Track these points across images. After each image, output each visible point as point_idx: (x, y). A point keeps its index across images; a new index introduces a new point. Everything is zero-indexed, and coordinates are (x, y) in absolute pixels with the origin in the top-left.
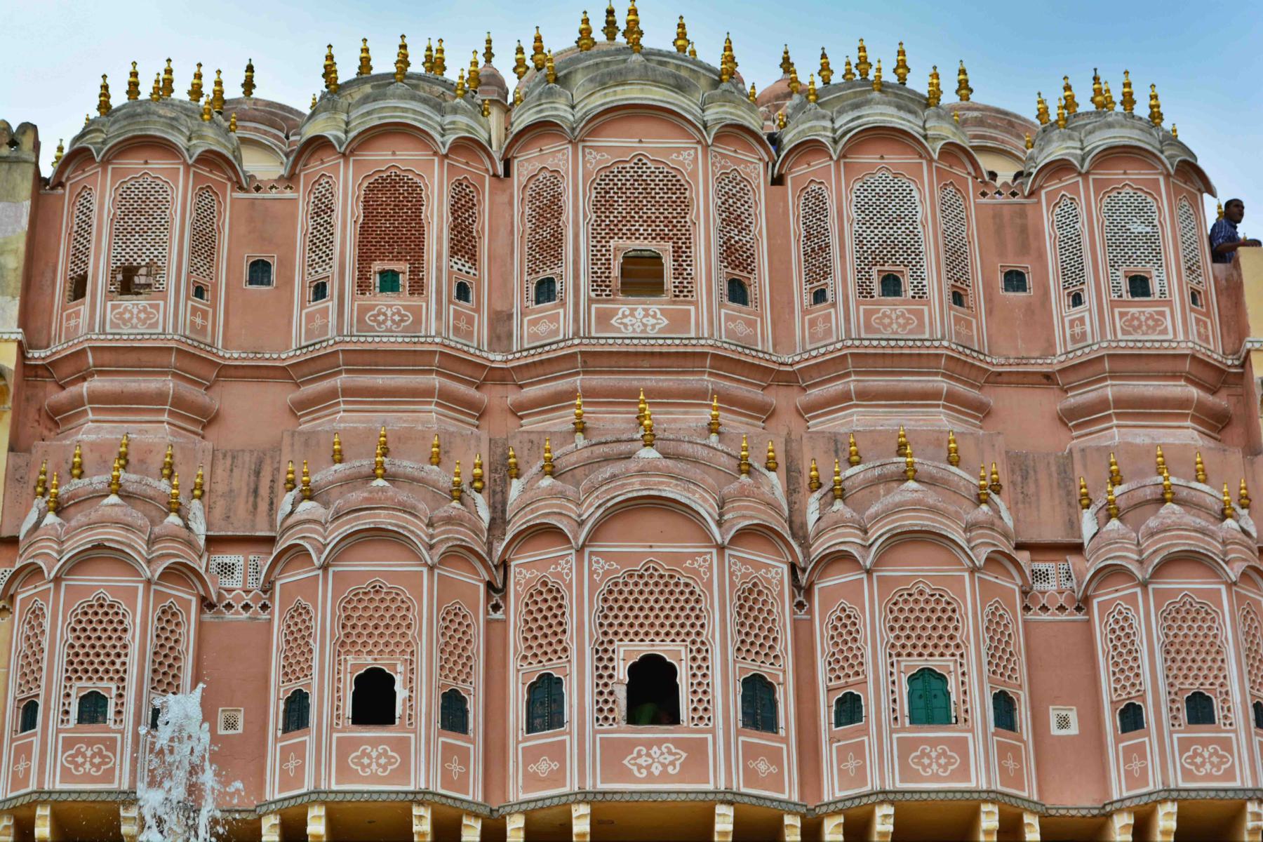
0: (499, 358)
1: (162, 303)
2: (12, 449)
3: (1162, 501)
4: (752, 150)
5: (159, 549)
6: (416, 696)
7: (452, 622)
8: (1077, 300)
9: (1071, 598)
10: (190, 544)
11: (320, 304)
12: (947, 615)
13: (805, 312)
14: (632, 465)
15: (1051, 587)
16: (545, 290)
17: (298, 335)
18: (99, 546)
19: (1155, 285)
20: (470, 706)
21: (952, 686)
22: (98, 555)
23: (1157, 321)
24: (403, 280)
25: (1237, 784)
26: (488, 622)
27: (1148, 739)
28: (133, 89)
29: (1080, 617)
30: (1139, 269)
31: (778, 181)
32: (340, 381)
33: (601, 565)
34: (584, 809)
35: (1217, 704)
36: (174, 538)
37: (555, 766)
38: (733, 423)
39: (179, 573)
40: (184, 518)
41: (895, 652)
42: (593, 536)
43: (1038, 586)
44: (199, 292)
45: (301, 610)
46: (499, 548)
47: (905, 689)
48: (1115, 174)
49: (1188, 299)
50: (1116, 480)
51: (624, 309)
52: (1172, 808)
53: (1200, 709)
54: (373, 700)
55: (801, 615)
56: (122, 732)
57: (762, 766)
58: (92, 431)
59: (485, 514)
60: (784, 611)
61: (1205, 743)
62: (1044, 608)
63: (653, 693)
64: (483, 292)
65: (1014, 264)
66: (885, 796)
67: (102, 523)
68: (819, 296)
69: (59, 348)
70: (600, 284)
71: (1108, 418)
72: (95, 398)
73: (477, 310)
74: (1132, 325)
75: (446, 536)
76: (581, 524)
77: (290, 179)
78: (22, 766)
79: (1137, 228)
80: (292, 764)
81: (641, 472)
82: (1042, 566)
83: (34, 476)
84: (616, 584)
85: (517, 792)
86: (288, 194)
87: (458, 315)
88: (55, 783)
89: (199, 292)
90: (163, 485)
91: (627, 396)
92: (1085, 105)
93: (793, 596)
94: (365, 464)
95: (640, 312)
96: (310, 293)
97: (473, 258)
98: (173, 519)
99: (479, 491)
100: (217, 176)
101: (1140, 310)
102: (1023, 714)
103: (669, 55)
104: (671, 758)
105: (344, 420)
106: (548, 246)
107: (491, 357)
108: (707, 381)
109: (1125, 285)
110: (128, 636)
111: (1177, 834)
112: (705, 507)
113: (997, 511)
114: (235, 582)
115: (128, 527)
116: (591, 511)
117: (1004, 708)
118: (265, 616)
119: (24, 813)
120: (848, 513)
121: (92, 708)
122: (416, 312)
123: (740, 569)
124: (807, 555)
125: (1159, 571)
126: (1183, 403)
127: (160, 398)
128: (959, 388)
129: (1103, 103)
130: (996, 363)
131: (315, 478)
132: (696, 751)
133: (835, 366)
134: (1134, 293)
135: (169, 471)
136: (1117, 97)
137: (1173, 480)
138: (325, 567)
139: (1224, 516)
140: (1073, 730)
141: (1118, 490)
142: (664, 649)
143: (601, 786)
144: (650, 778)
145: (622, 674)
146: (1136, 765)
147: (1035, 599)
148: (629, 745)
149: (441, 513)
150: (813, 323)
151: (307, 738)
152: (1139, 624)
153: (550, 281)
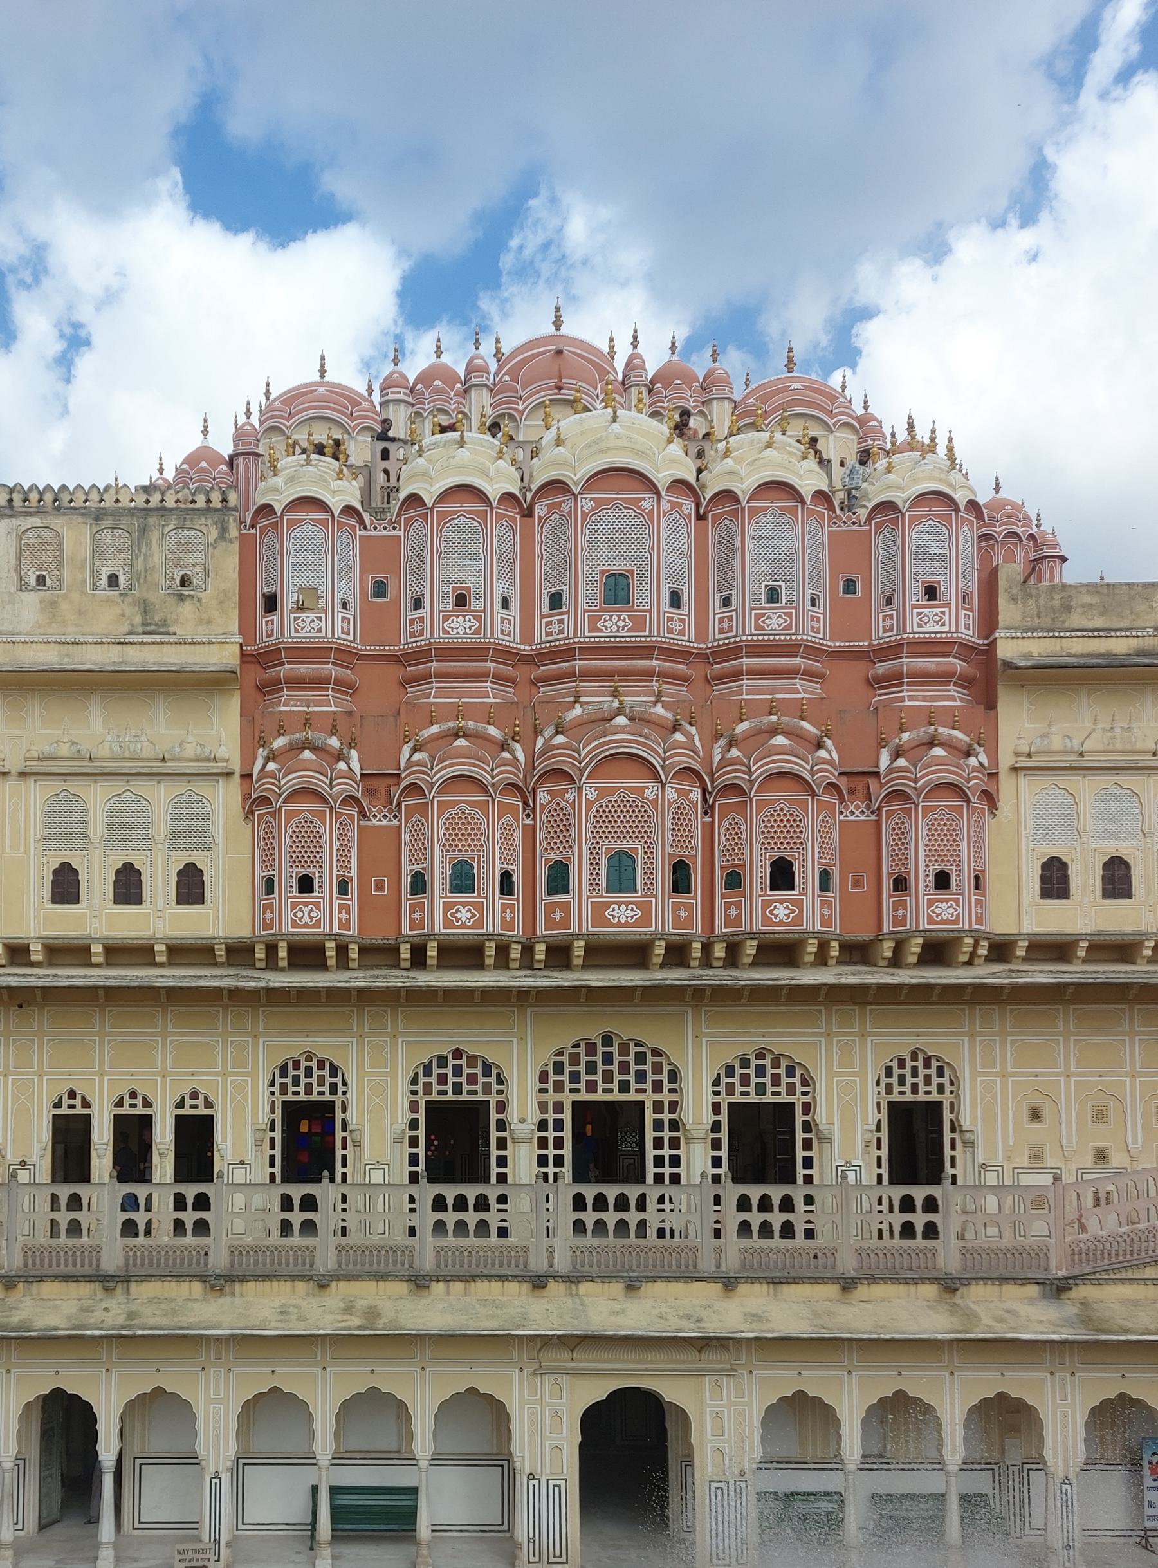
0: (527, 648)
1: (323, 616)
20: (515, 879)
40: (348, 764)
54: (463, 879)
56: (323, 898)
59: (521, 757)
63: (622, 873)
66: (751, 935)
69: (263, 641)
78: (268, 916)
80: (417, 915)
84: (601, 806)
88: (287, 928)
93: (703, 807)
99: (517, 742)
104: (632, 913)
107: (522, 647)
110: (322, 842)
118: (395, 822)
121: (306, 884)
132: (645, 908)
144: (619, 925)
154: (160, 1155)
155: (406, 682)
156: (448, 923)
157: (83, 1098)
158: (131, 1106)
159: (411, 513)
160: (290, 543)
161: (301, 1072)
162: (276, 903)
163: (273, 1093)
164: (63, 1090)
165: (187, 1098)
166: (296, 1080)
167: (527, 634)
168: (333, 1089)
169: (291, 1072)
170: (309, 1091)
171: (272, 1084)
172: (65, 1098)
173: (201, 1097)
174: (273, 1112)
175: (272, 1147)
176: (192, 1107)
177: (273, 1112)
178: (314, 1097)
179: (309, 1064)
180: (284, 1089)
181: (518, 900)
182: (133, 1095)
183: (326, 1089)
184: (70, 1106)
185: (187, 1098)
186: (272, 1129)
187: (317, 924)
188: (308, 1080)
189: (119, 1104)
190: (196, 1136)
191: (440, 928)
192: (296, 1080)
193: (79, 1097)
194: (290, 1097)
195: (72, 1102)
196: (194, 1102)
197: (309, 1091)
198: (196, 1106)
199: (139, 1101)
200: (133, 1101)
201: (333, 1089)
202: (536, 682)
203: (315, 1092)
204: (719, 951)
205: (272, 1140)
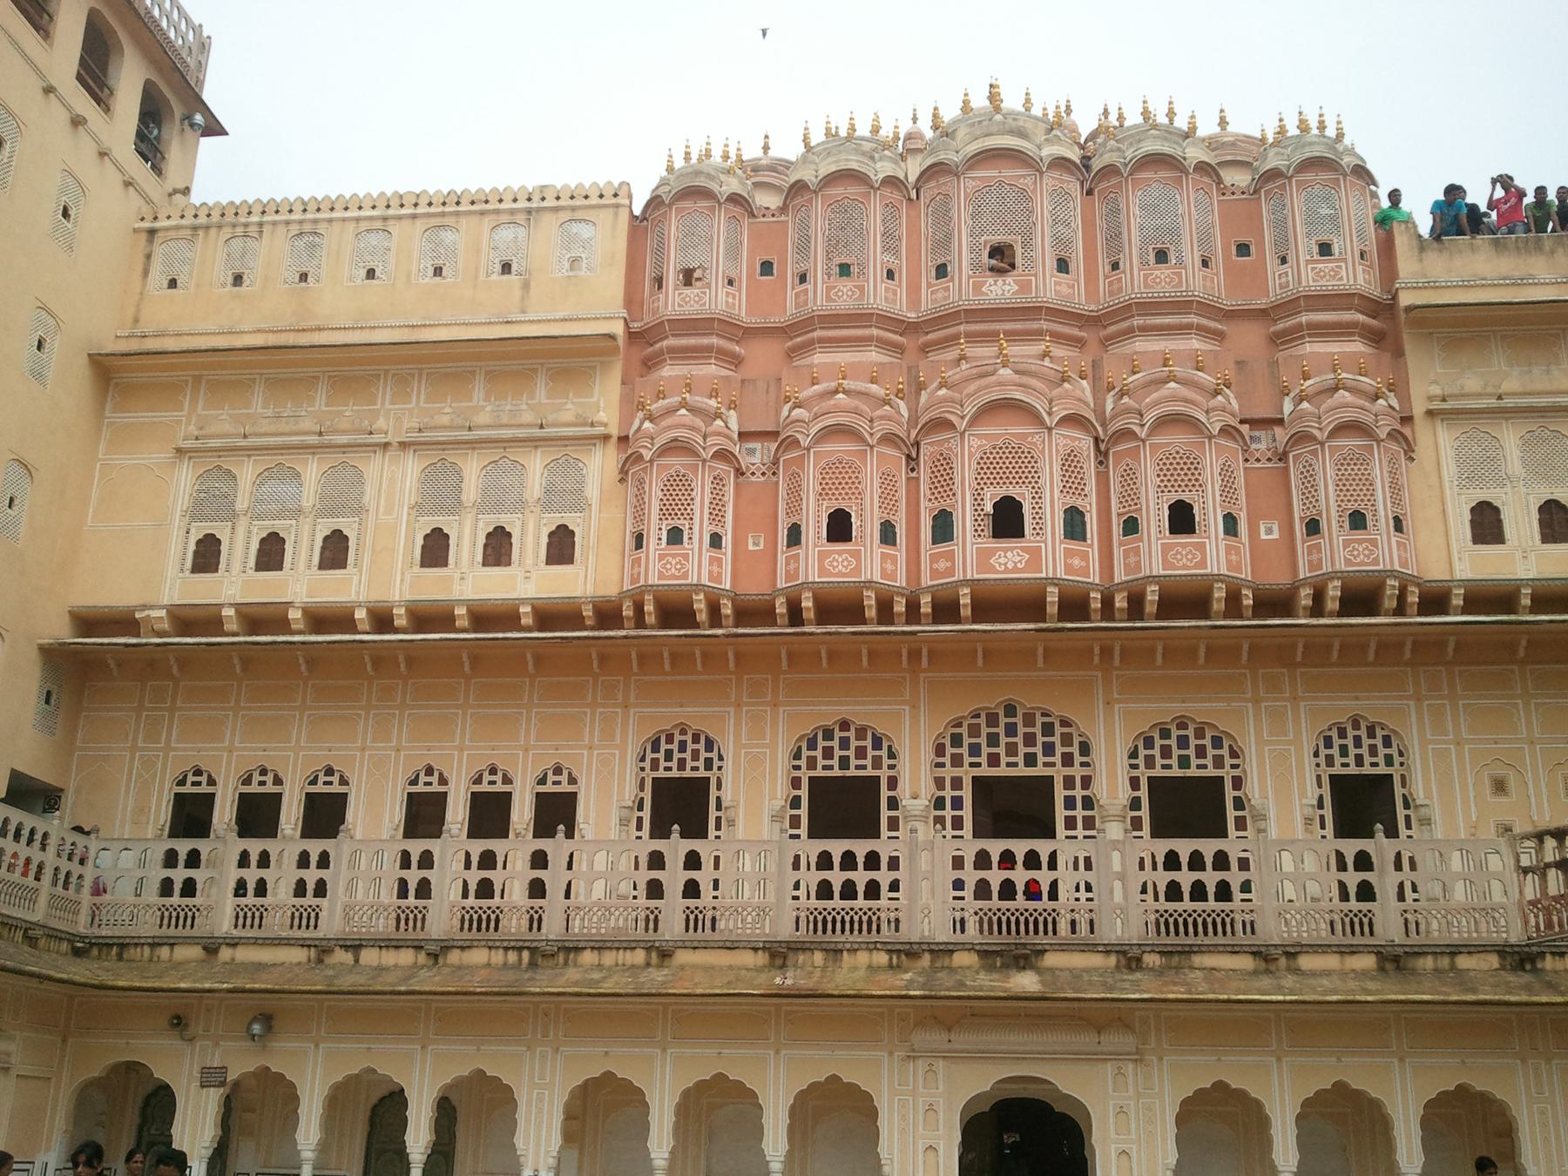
2: (623, 383)
3: (1336, 389)
4: (1072, 174)
5: (710, 441)
6: (866, 525)
7: (887, 479)
8: (1284, 261)
9: (1275, 453)
10: (730, 438)
11: (803, 287)
12: (1192, 467)
13: (1106, 277)
14: (993, 378)
15: (1263, 446)
16: (941, 271)
17: (791, 308)
18: (675, 440)
19: (1336, 249)
21: (1196, 511)
22: (676, 447)
23: (1335, 274)
24: (855, 269)
25: (1381, 567)
26: (908, 479)
27: (1322, 541)
28: (687, 156)
29: (1281, 465)
30: (1325, 238)
31: (1090, 192)
32: (818, 334)
33: (976, 442)
34: (967, 591)
35: (1369, 517)
36: (719, 434)
37: (949, 564)
38: (1059, 351)
39: (723, 455)
41: (1161, 490)
42: (973, 422)
43: (1254, 446)
44: (730, 283)
45: (795, 475)
46: (913, 434)
47: (1167, 513)
48: (1309, 176)
49: (1357, 256)
50: (1306, 377)
51: (991, 281)
52: (1338, 583)
53: (1358, 520)
54: (839, 528)
55: (1102, 469)
57: (1076, 562)
58: (668, 371)
60: (1090, 468)
61: (1360, 542)
62: (1258, 460)
63: (1007, 520)
64: (903, 275)
65: (1242, 240)
67: (676, 426)
68: (1115, 266)
69: (648, 319)
70: (975, 266)
71: (1303, 337)
72: (672, 350)
73: (900, 285)
74: (1319, 274)
75: (880, 428)
76: (963, 418)
77: (783, 209)
78: (636, 571)
79: (1325, 211)
80: (792, 567)
81: (1001, 384)
82: (1257, 433)
83: (636, 400)
85: (926, 581)
86: (783, 218)
87: (887, 289)
88: (654, 580)
89: (730, 283)
90: (713, 403)
91: (990, 337)
92: (1293, 131)
94: (834, 384)
95: (1000, 282)
96: (797, 280)
97: (896, 252)
98: (719, 422)
100: (738, 209)
101: (1326, 266)
102: (1243, 527)
103: (1019, 114)
105: (819, 358)
106: (944, 242)
108: (1045, 325)
109: (1316, 249)
111: (1341, 600)
112: (1040, 406)
113: (1227, 398)
114: (757, 459)
115: (692, 428)
116: (970, 410)
117: (1231, 524)
118: (774, 479)
119: (637, 598)
120: (1132, 403)
121: (675, 536)
122: (861, 289)
123: (1062, 441)
124: (1105, 431)
125: (1332, 435)
126: (1355, 324)
127: (709, 349)
128: (1204, 322)
129: (1303, 127)
130: (1228, 303)
131: (803, 395)
132: (1035, 554)
133: (1126, 311)
134: (1322, 253)
135: (714, 394)
136: (1313, 124)
137: (1344, 375)
138: (808, 449)
139: (1377, 398)
140: (1275, 535)
141: (1309, 383)
142: (1014, 491)
143: (976, 576)
144: (1007, 570)
145: (989, 508)
146: (1315, 557)
147: (1252, 454)
148: (992, 552)
149: (879, 413)
150: (1111, 284)
151: (799, 551)
152: (1318, 467)
153: (945, 265)
154: (517, 835)
155: (792, 354)
156: (822, 571)
157: (441, 775)
158: (491, 783)
159: (799, 200)
160: (674, 227)
161: (675, 747)
162: (643, 556)
163: (643, 769)
164: (420, 765)
165: (550, 773)
166: (669, 755)
167: (914, 302)
168: (709, 764)
169: (664, 747)
170: (682, 765)
171: (643, 759)
172: (422, 774)
173: (565, 773)
174: (642, 788)
175: (639, 828)
176: (555, 783)
177: (642, 788)
178: (688, 773)
179: (683, 738)
180: (655, 765)
181: (900, 552)
182: (493, 771)
183: (701, 764)
184: (426, 784)
185: (550, 773)
186: (640, 808)
187: (685, 576)
188: (682, 755)
189: (478, 781)
190: (556, 813)
191: (814, 577)
192: (669, 755)
193: (436, 774)
194: (661, 774)
195: (428, 779)
196: (557, 778)
197: (682, 765)
198: (559, 783)
199: (498, 778)
200: (493, 778)
201: (709, 764)
202: (925, 350)
203: (688, 767)
204: (1120, 602)
205: (640, 820)
